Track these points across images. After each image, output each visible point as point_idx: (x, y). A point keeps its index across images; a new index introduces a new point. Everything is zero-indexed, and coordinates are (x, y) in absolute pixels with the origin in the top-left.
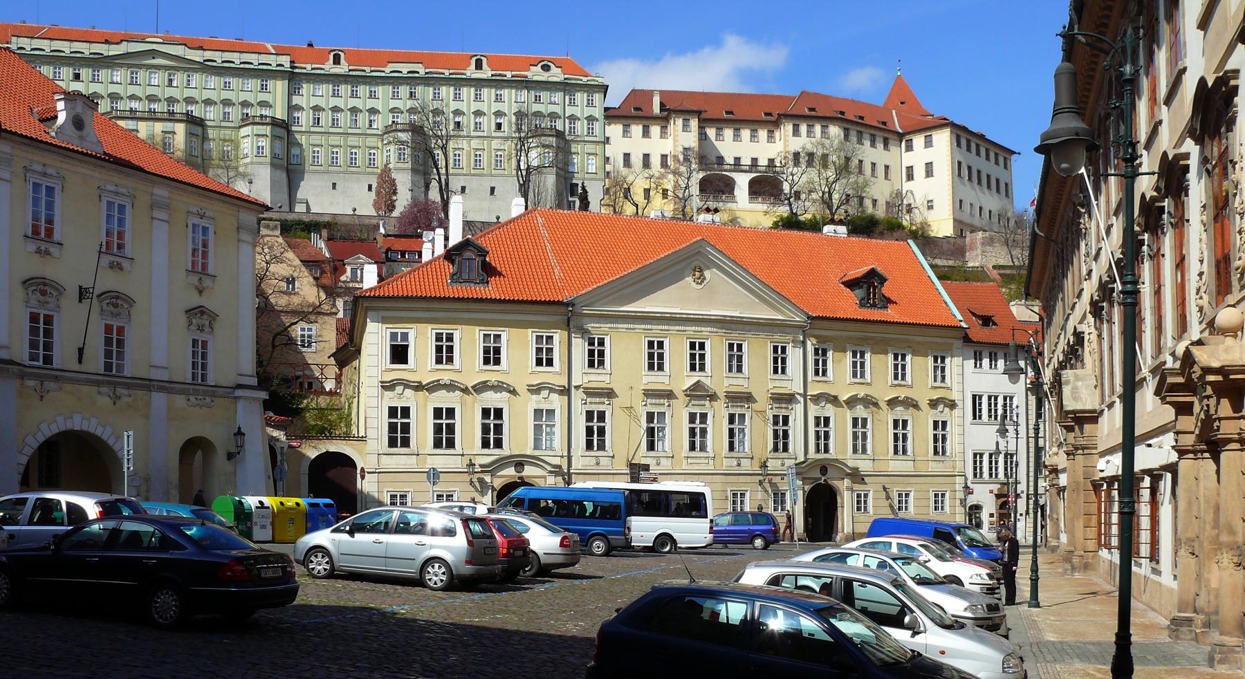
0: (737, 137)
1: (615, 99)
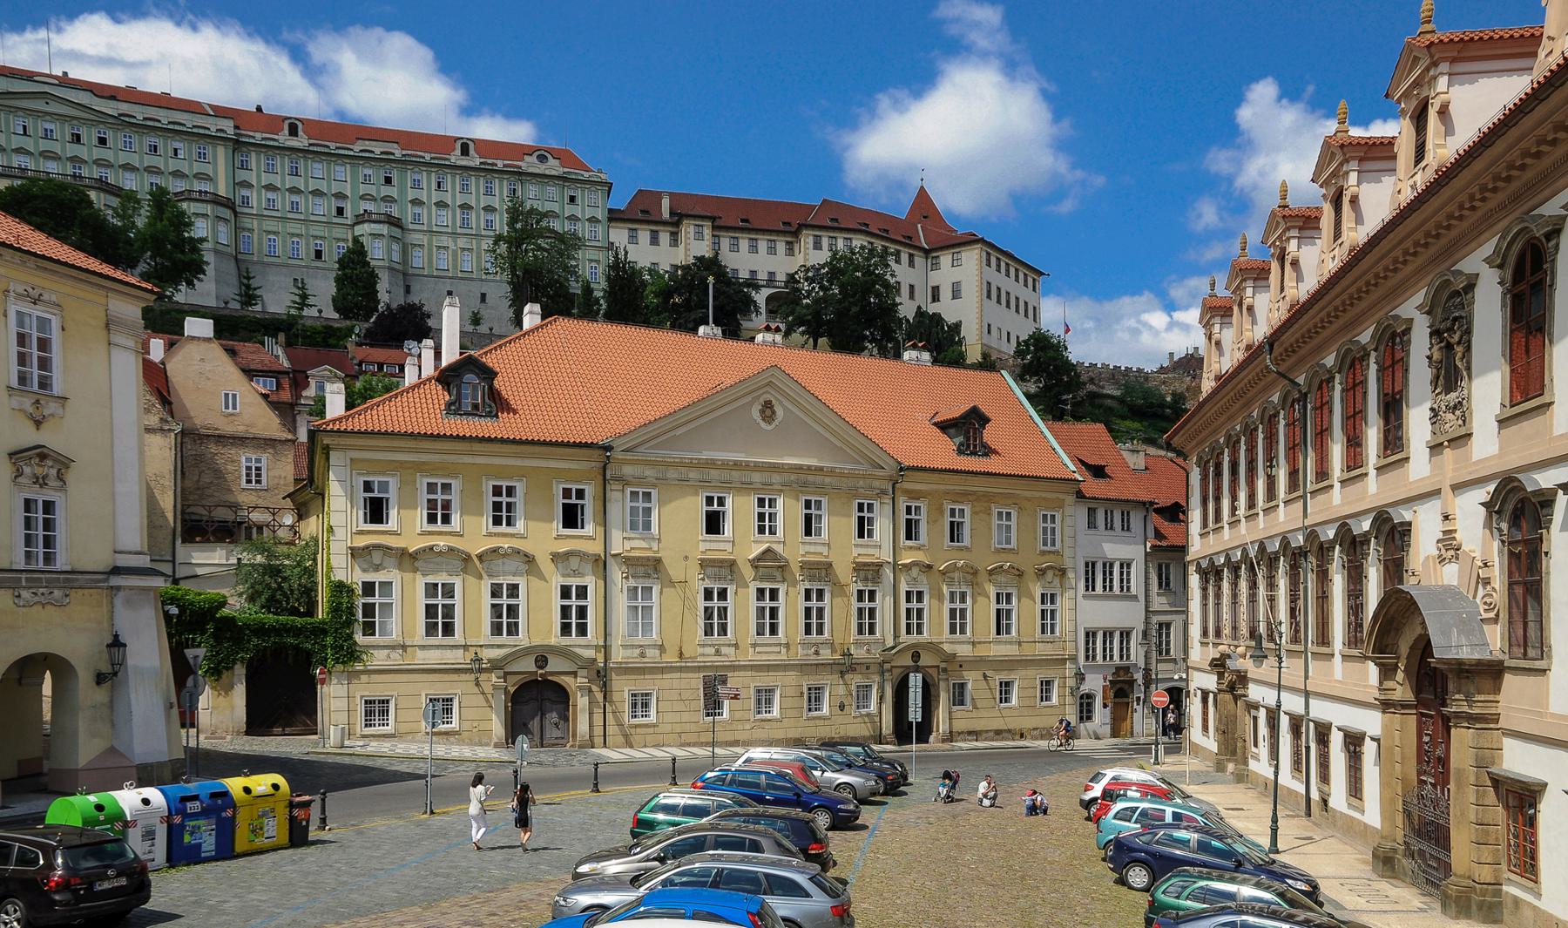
0: (754, 249)
1: (620, 201)
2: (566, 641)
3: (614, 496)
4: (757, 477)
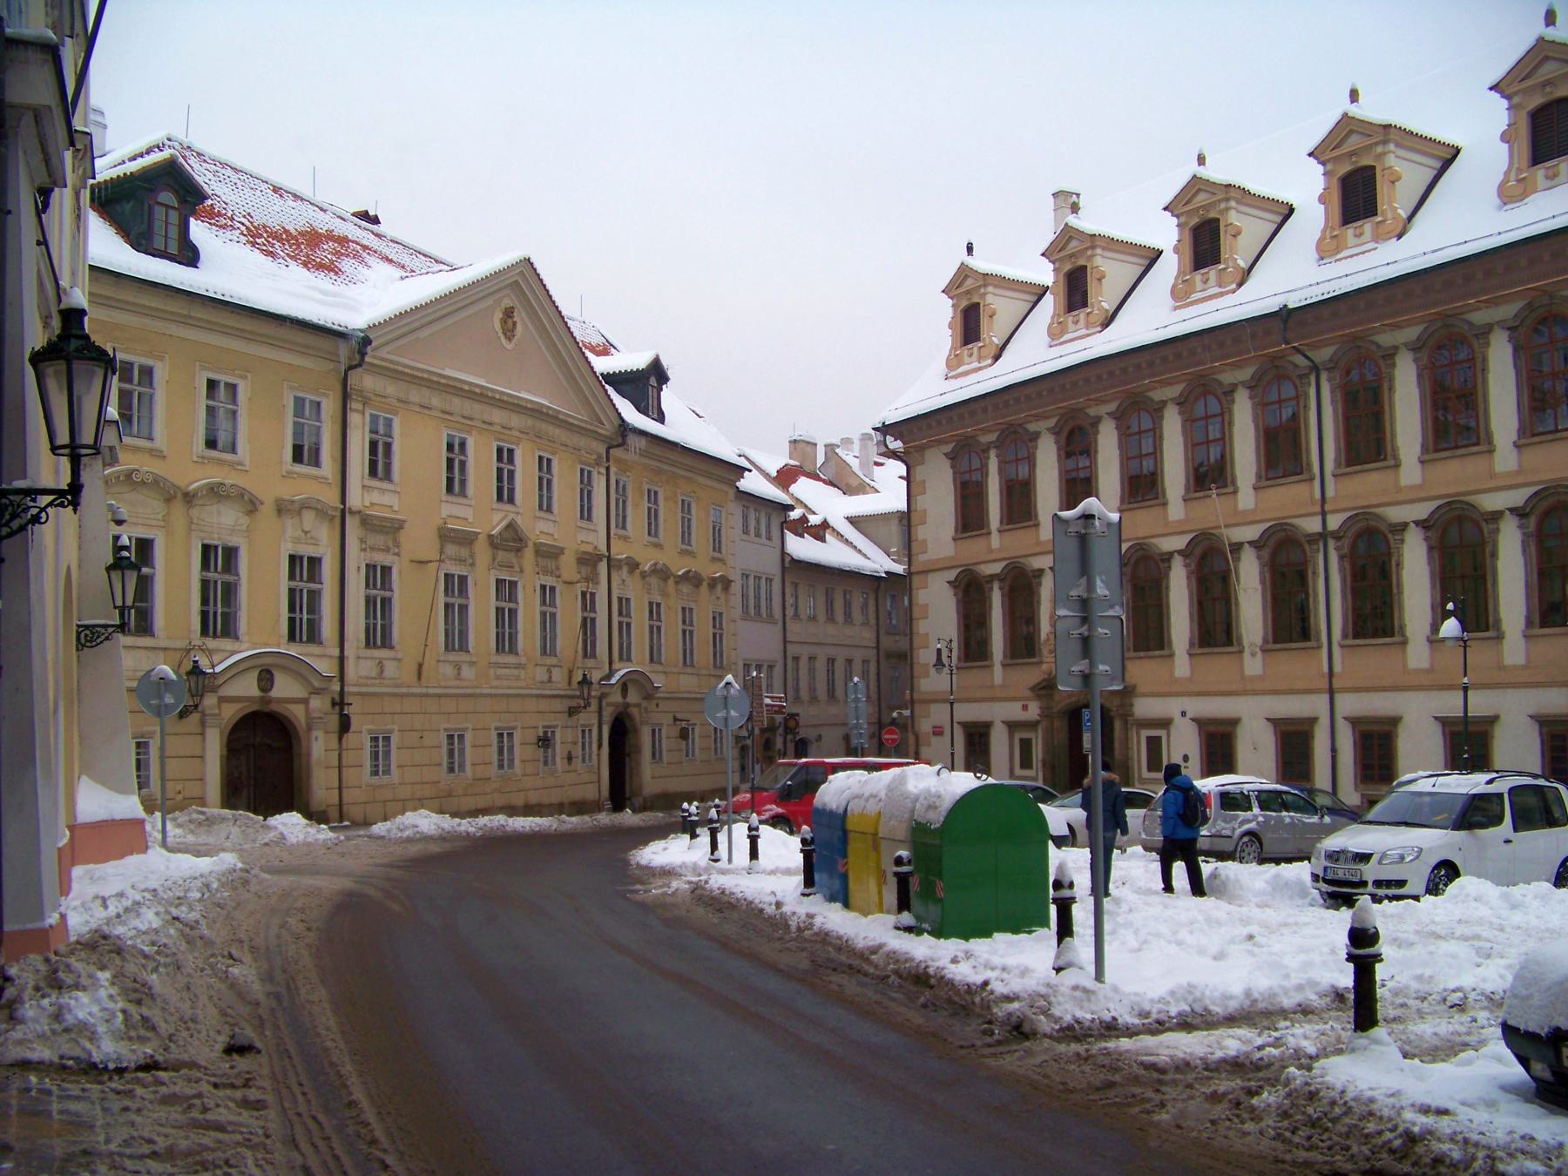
2: (294, 650)
3: (354, 419)
4: (497, 416)
